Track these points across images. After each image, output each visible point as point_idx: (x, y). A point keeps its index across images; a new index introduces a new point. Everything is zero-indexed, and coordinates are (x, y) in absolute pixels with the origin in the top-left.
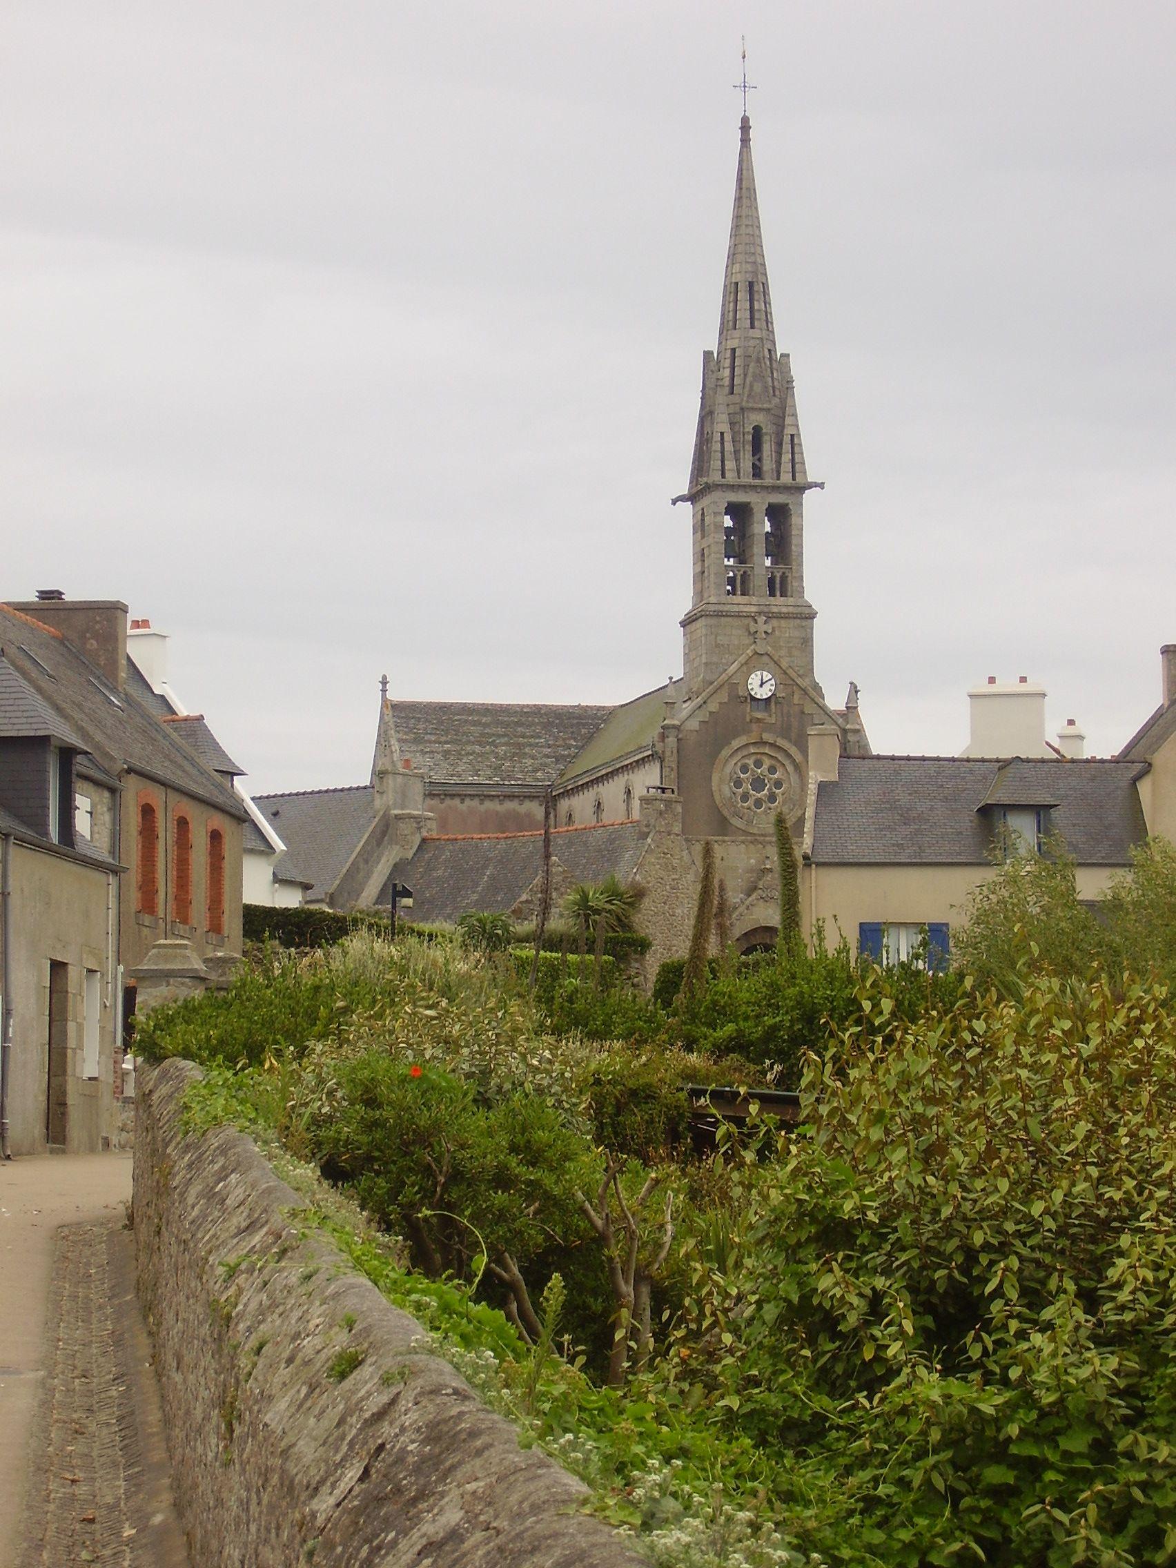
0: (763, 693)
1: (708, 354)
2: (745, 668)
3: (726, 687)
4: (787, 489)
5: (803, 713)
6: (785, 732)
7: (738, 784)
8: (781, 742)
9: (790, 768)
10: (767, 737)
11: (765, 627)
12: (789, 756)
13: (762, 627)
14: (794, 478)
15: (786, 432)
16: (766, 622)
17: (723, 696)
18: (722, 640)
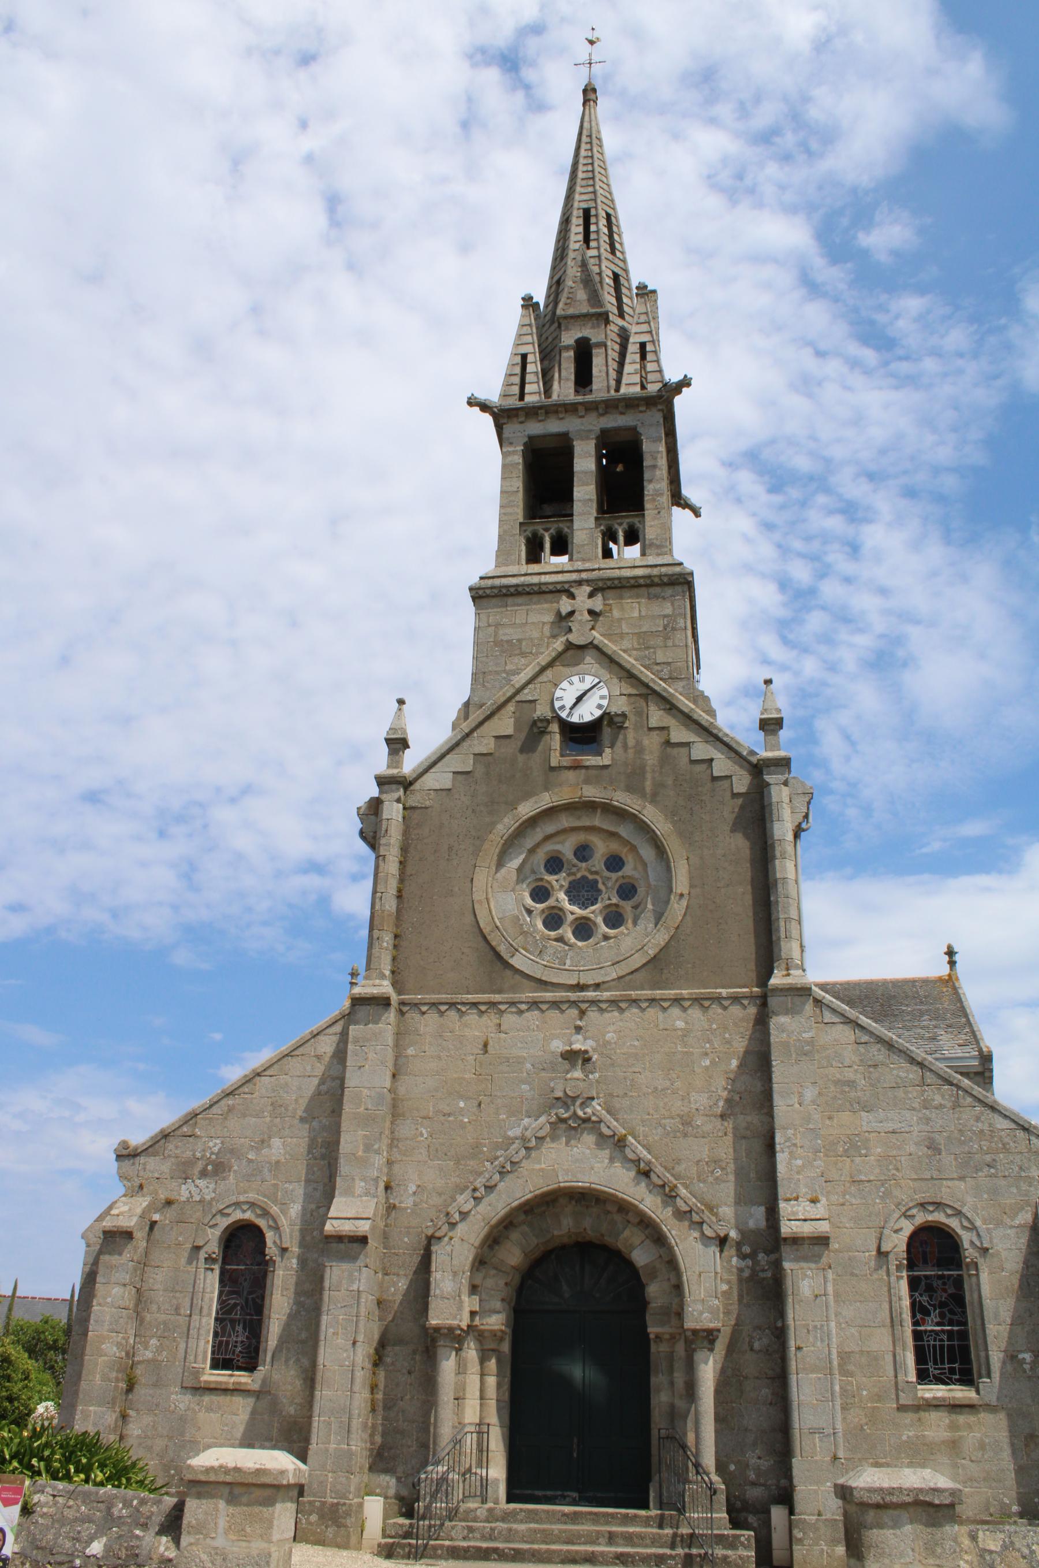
0: (587, 713)
1: (528, 303)
2: (549, 674)
3: (511, 707)
4: (630, 403)
5: (668, 743)
6: (634, 782)
7: (540, 894)
8: (621, 799)
9: (647, 852)
10: (591, 792)
11: (590, 604)
12: (644, 828)
13: (583, 601)
14: (643, 387)
15: (631, 340)
16: (591, 595)
17: (505, 724)
18: (509, 634)
